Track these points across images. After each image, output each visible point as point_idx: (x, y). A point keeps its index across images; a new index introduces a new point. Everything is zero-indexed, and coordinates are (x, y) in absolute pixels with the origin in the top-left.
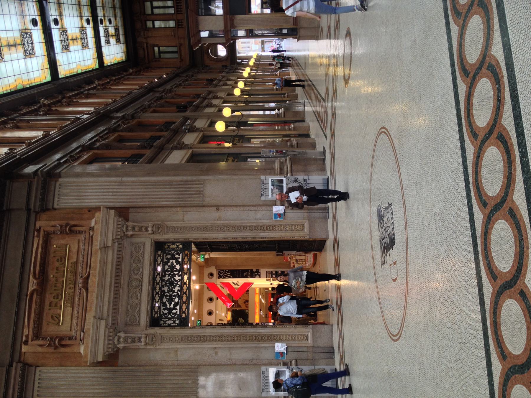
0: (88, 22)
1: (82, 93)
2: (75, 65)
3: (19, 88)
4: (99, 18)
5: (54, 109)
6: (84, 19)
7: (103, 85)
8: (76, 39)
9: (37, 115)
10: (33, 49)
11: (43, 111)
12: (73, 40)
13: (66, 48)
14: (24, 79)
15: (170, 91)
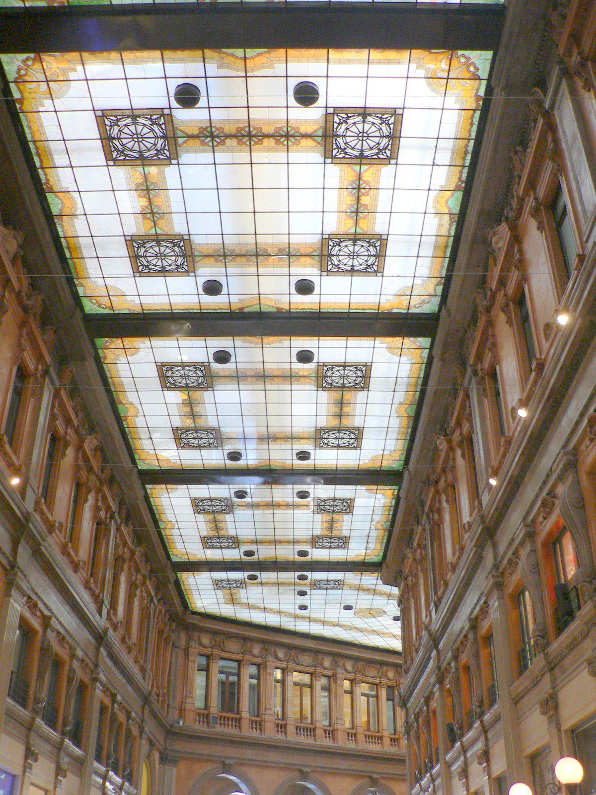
0: (249, 553)
1: (112, 517)
2: (170, 517)
3: (119, 406)
4: (257, 573)
5: (70, 452)
6: (253, 548)
7: (132, 557)
8: (217, 529)
9: (53, 418)
10: (189, 446)
11: (66, 433)
12: (215, 521)
13: (198, 505)
14: (137, 419)
15: (95, 680)
